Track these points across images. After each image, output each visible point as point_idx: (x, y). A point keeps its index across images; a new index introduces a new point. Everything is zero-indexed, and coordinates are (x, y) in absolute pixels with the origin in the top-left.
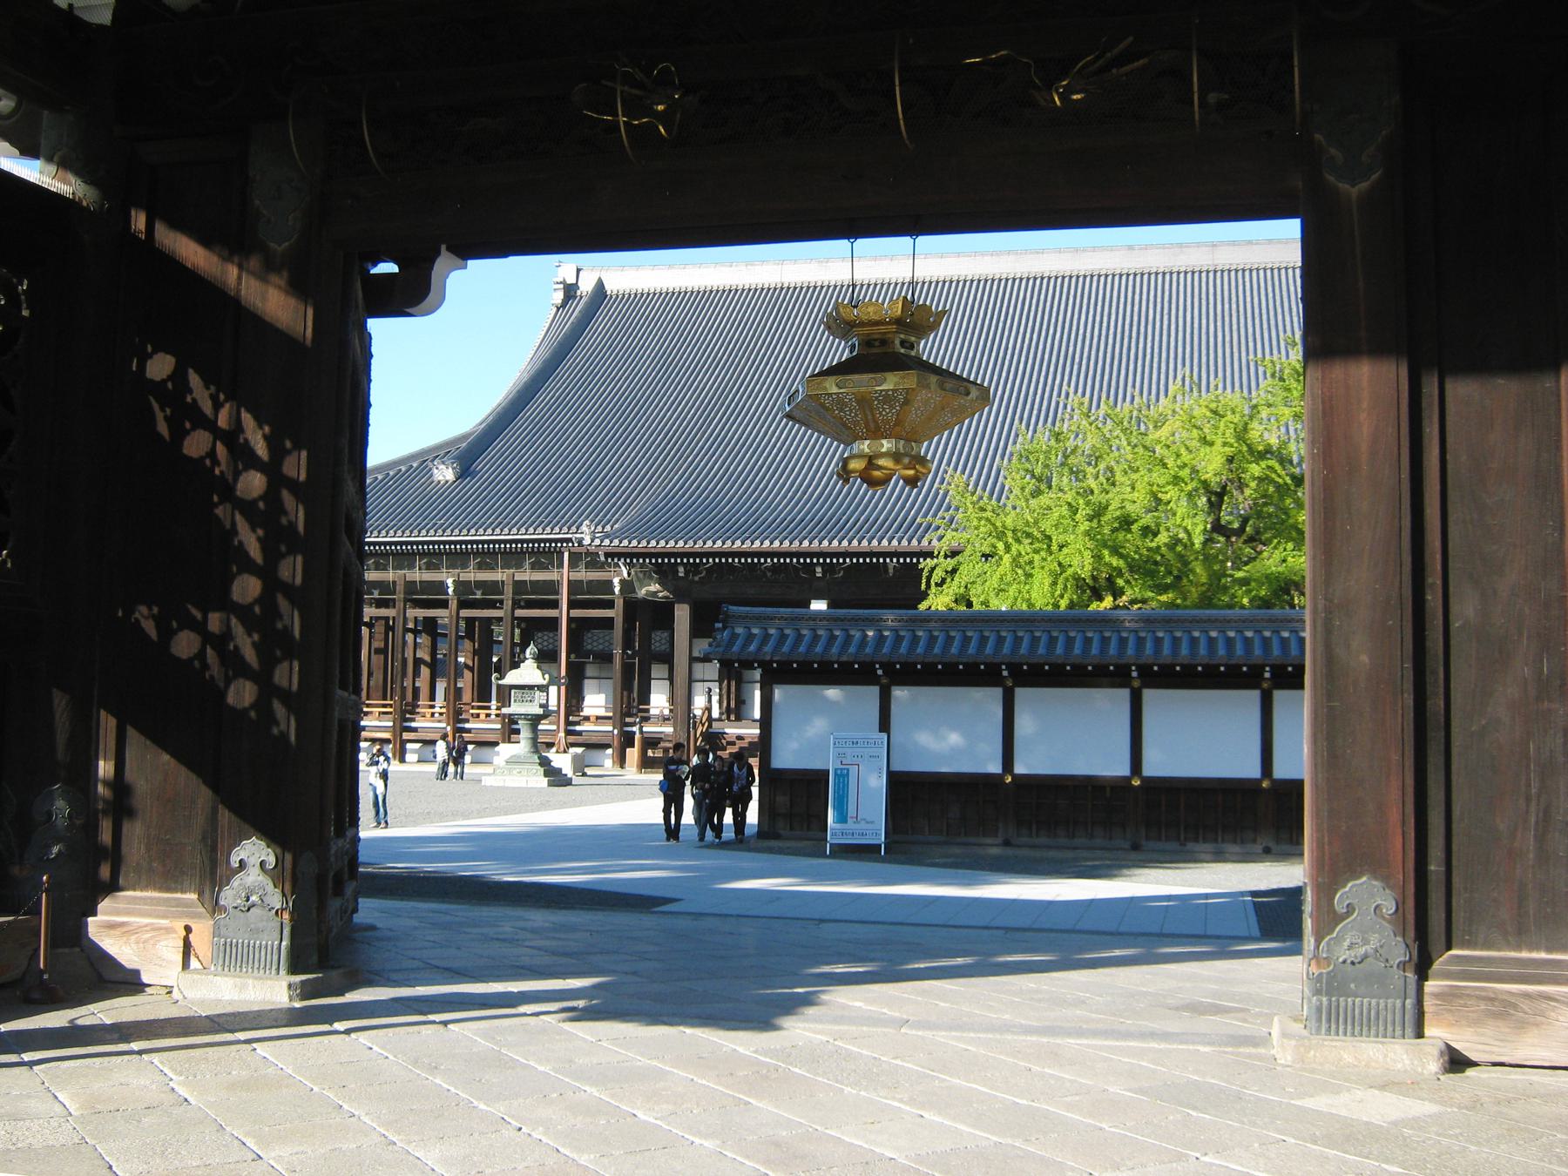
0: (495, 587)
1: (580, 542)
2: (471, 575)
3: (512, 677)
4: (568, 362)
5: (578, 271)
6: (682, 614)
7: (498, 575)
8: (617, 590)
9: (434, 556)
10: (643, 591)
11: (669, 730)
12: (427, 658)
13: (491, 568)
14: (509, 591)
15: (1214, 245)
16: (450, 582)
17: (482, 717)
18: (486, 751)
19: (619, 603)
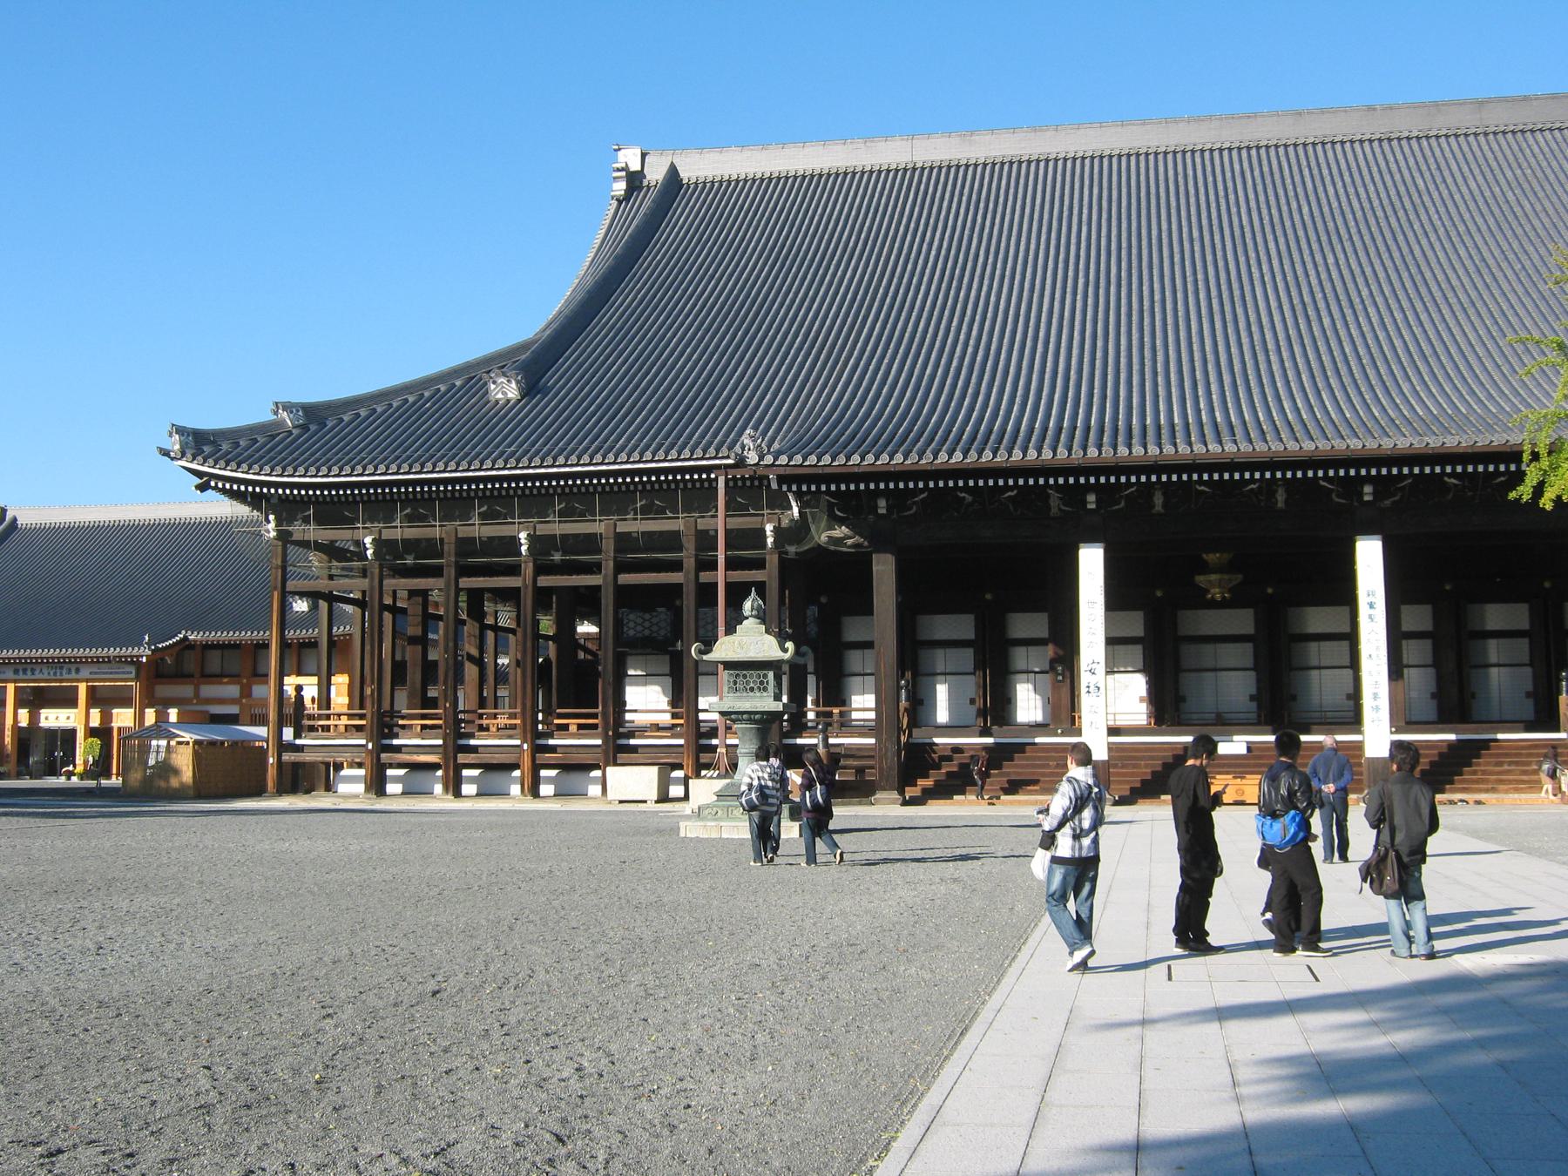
0: (590, 543)
1: (741, 463)
2: (556, 527)
3: (726, 648)
4: (646, 261)
5: (644, 156)
6: (884, 569)
7: (598, 526)
8: (770, 540)
9: (502, 499)
10: (824, 538)
11: (872, 741)
12: (475, 652)
13: (585, 513)
14: (608, 546)
15: (1481, 104)
16: (523, 536)
17: (573, 728)
18: (575, 779)
19: (773, 561)
